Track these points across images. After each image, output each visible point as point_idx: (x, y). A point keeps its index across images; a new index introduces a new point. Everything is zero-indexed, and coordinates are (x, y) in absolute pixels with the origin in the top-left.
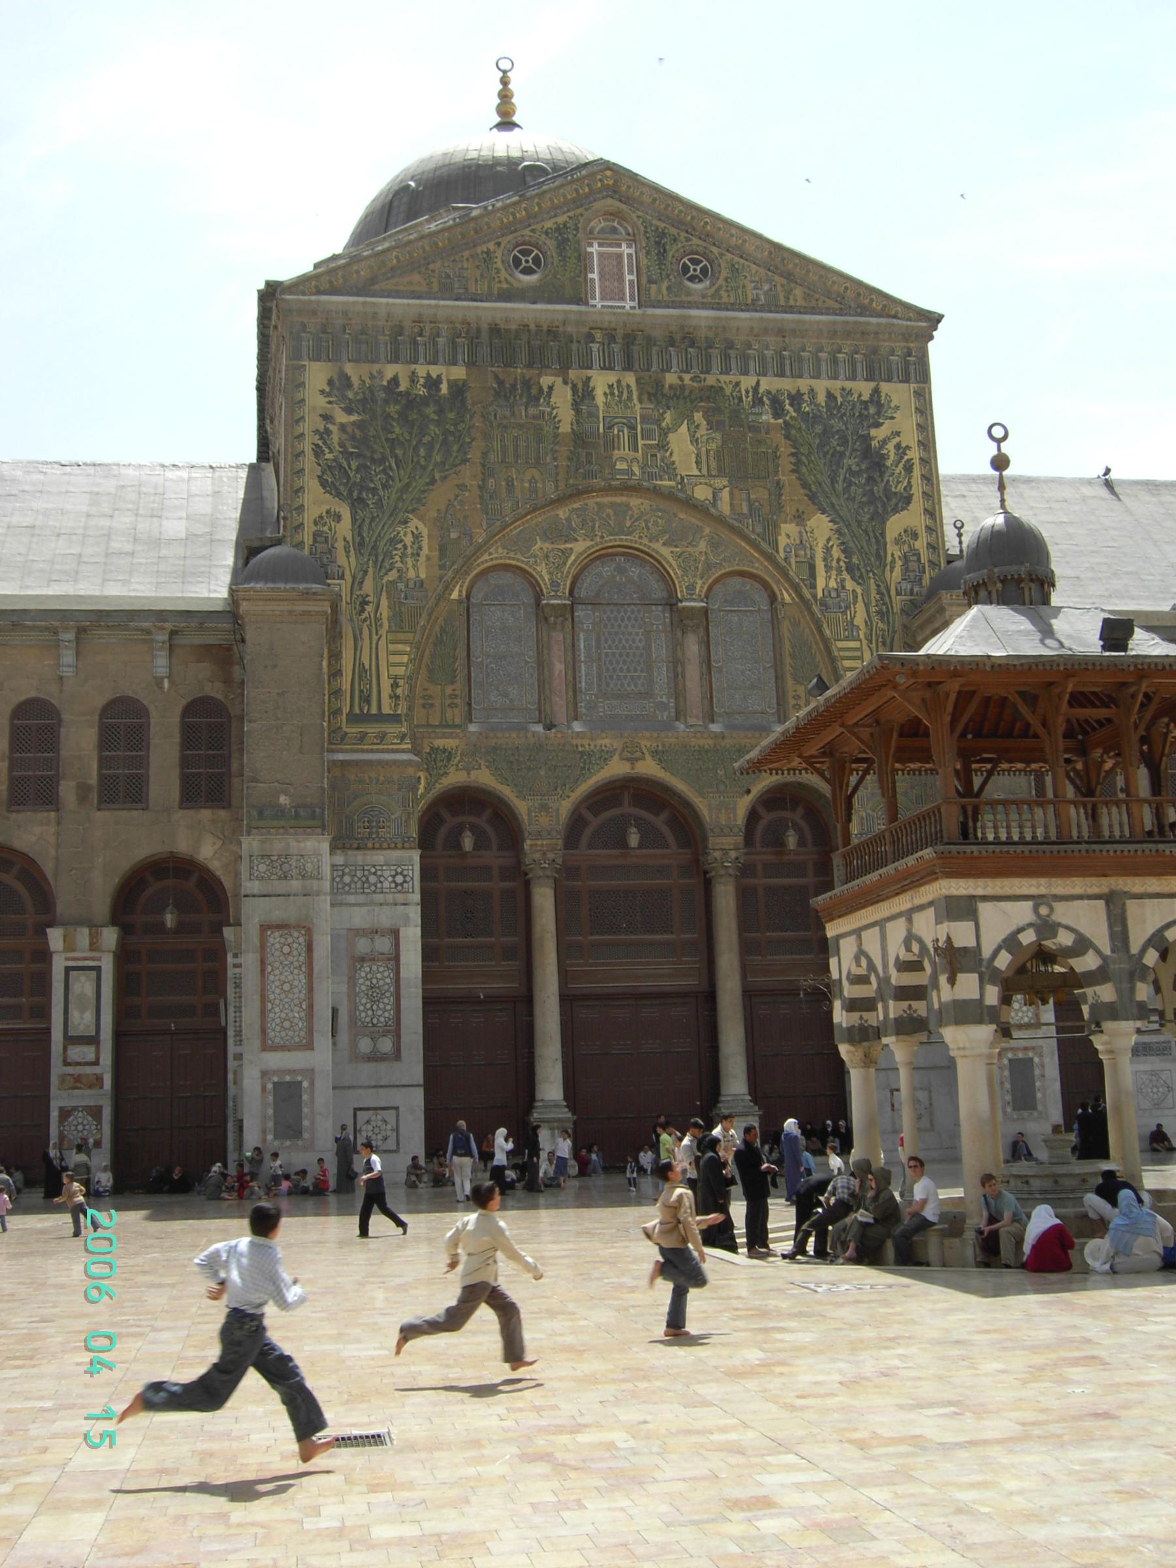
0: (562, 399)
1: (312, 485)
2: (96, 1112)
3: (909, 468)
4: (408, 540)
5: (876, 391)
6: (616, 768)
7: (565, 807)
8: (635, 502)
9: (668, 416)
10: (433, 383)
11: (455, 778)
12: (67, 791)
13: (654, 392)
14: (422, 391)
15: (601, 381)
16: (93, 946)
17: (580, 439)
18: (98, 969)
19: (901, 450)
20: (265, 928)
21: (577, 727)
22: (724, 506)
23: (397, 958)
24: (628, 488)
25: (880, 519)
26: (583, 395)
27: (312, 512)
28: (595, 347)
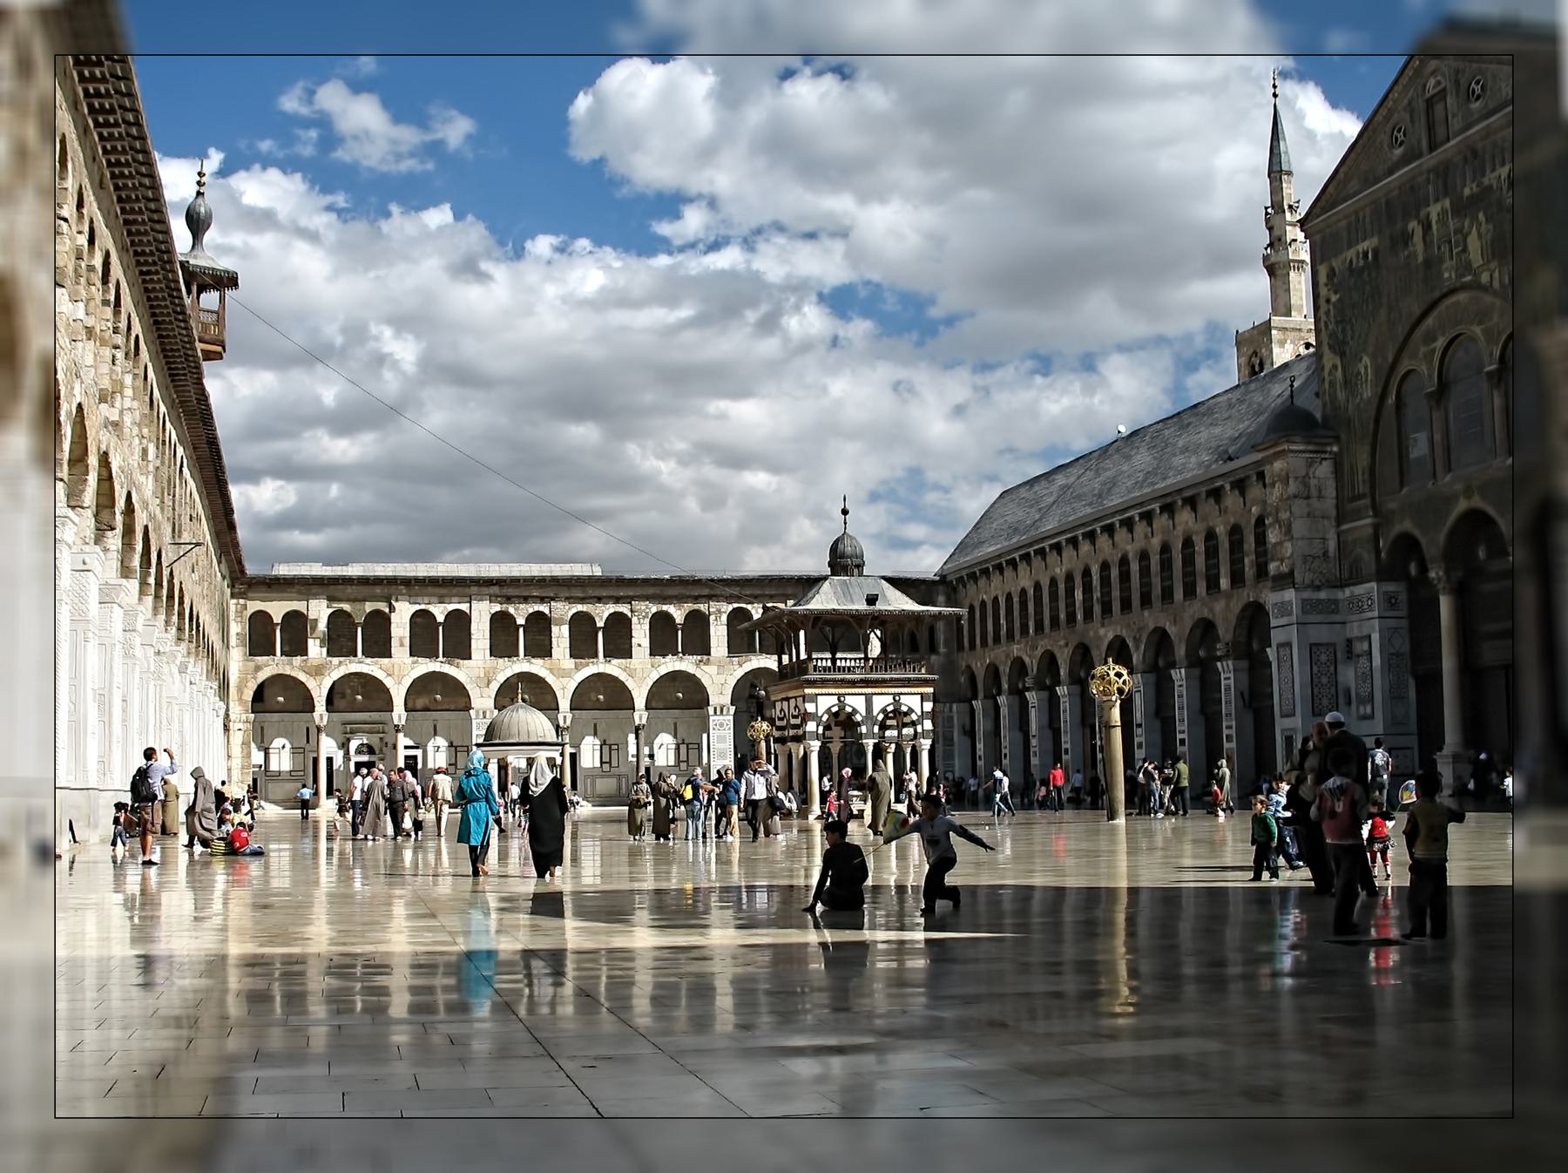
1: (1326, 349)
6: (1462, 505)
7: (1442, 538)
8: (1462, 297)
9: (1467, 224)
10: (1366, 254)
11: (1398, 528)
13: (1462, 208)
14: (1362, 263)
15: (1434, 211)
17: (1428, 263)
20: (1279, 646)
21: (1448, 478)
22: (1496, 284)
23: (1370, 653)
24: (1452, 291)
26: (1427, 227)
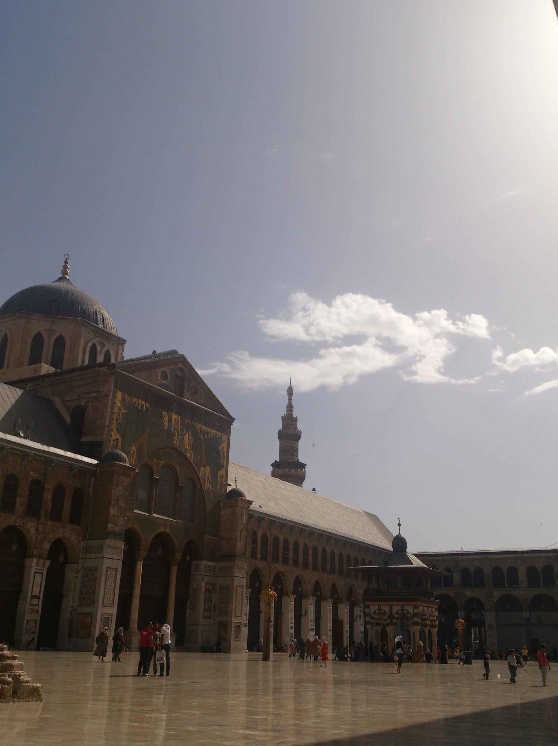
0: (166, 419)
1: (115, 429)
2: (36, 622)
3: (224, 458)
4: (132, 452)
5: (221, 436)
6: (162, 529)
7: (151, 538)
12: (42, 512)
14: (140, 408)
16: (43, 566)
18: (42, 573)
19: (224, 453)
25: (218, 470)
26: (170, 420)
27: (113, 438)
28: (174, 406)
